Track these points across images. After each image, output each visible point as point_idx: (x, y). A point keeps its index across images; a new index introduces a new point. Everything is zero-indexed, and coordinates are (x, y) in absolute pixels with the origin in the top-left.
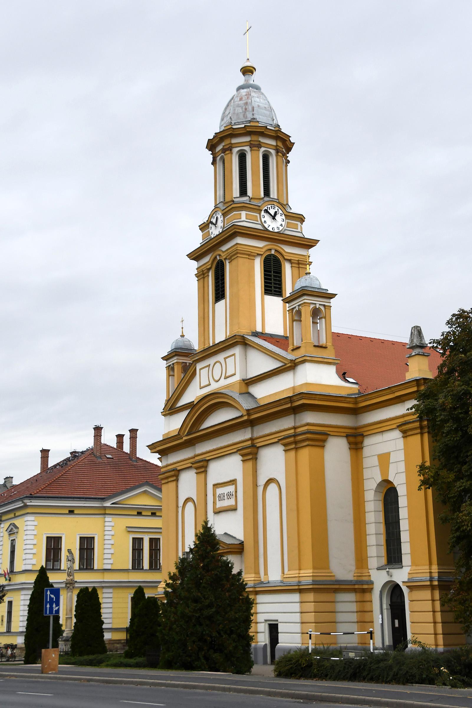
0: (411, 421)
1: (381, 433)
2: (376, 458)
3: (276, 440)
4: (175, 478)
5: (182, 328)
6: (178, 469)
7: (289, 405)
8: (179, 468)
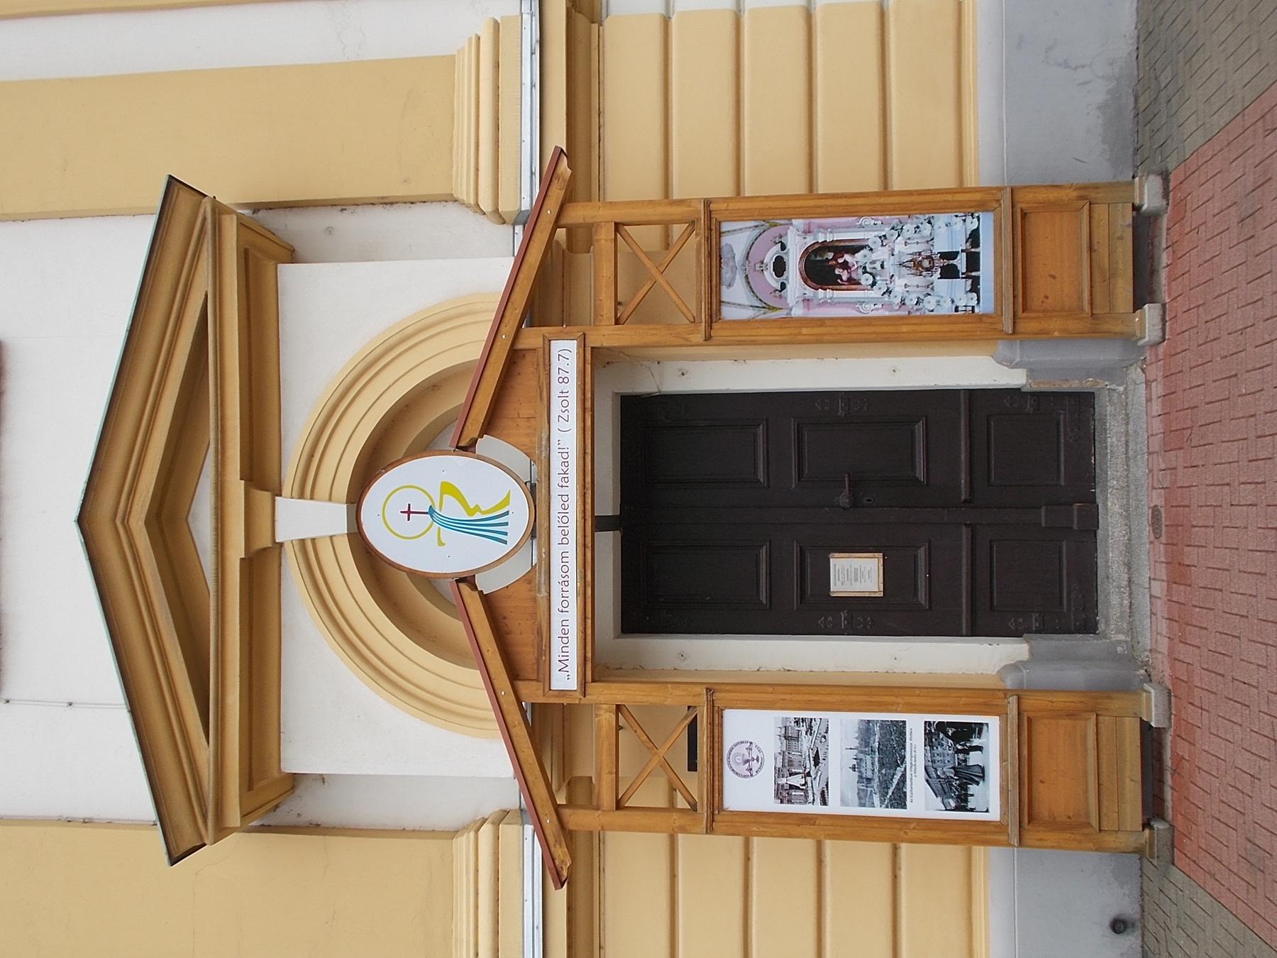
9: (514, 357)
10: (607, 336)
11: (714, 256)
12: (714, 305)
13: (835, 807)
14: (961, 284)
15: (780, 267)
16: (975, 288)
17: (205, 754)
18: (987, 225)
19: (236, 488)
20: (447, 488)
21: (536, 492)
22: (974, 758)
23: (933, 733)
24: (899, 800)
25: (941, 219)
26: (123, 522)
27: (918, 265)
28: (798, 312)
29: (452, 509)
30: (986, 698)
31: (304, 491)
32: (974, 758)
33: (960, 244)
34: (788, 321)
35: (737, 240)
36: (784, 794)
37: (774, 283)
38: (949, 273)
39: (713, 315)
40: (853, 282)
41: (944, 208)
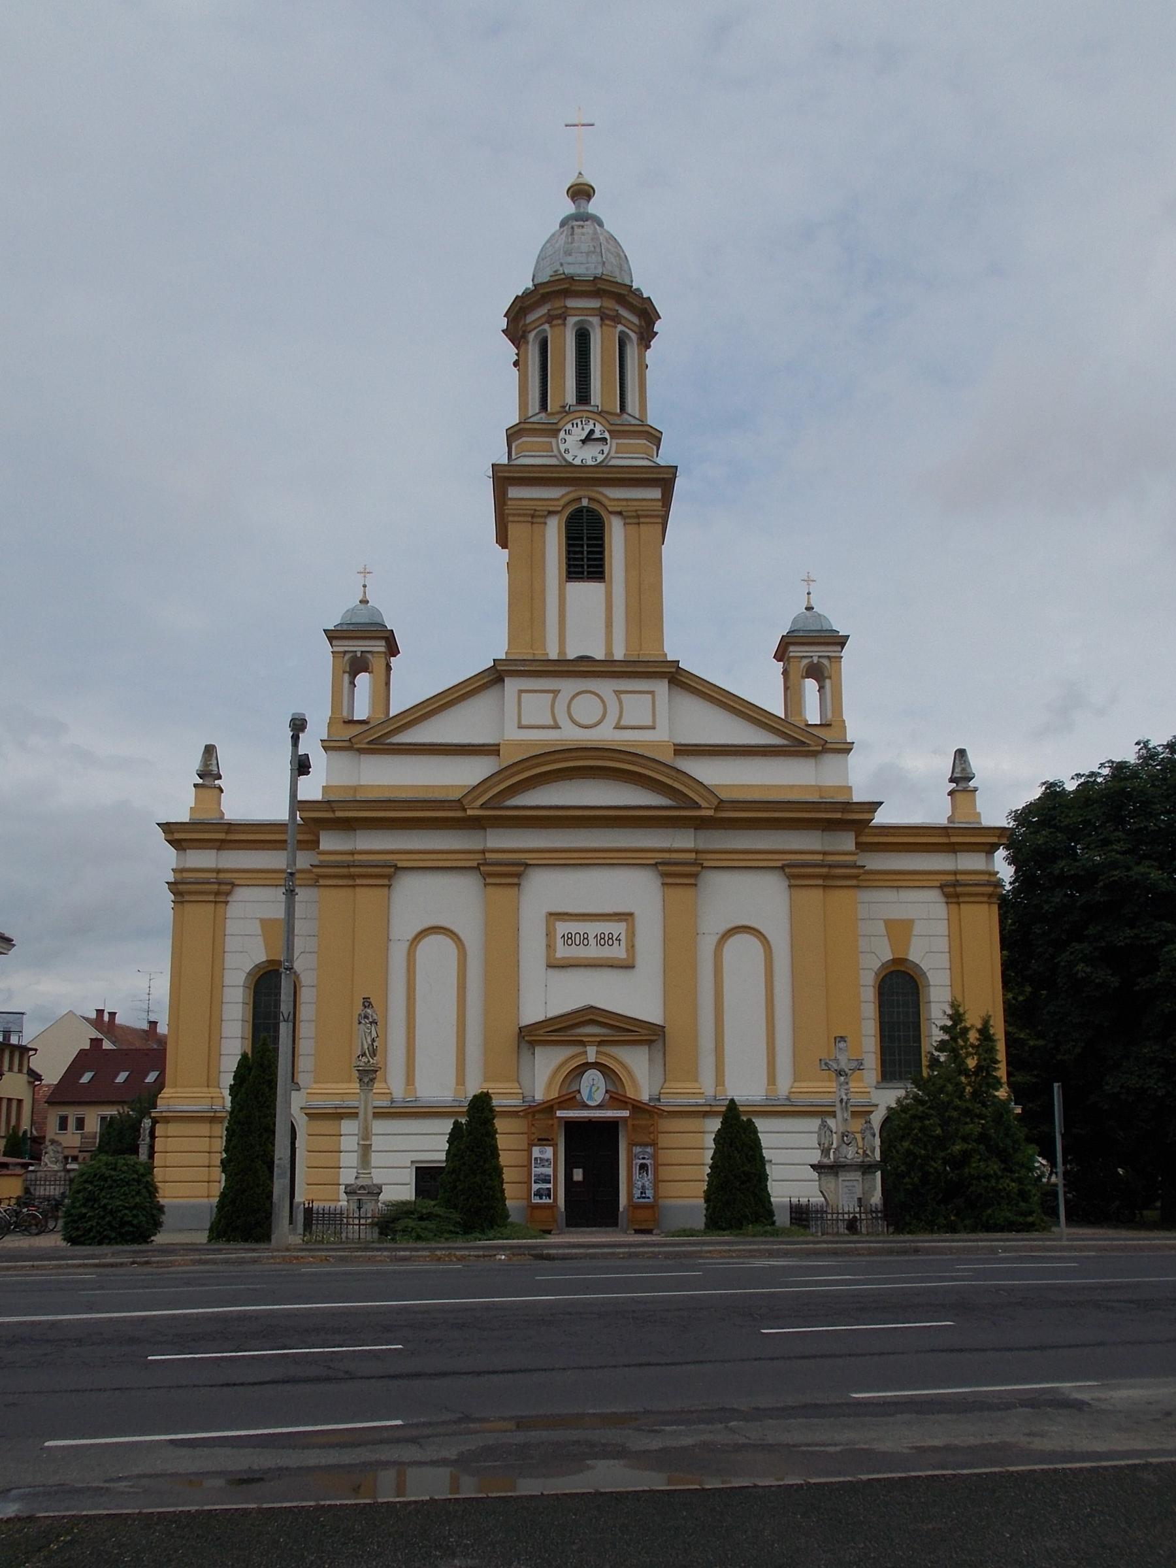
0: (971, 882)
1: (895, 889)
2: (882, 923)
3: (779, 864)
4: (385, 882)
5: (365, 586)
6: (399, 866)
7: (839, 816)
8: (400, 864)
9: (626, 1103)
10: (630, 1122)
11: (646, 1145)
12: (636, 1145)
13: (533, 1169)
14: (639, 1196)
15: (644, 1158)
16: (638, 1198)
17: (541, 1032)
18: (651, 1200)
19: (598, 1039)
20: (598, 1088)
21: (600, 1107)
22: (544, 1197)
23: (549, 1189)
24: (535, 1183)
25: (652, 1191)
26: (590, 1020)
27: (643, 1187)
28: (634, 1162)
29: (594, 1089)
30: (555, 1199)
31: (597, 1052)
32: (544, 1197)
33: (647, 1195)
34: (632, 1160)
35: (649, 1150)
36: (536, 1159)
37: (641, 1157)
38: (642, 1193)
39: (634, 1145)
40: (640, 1174)
41: (655, 1191)
